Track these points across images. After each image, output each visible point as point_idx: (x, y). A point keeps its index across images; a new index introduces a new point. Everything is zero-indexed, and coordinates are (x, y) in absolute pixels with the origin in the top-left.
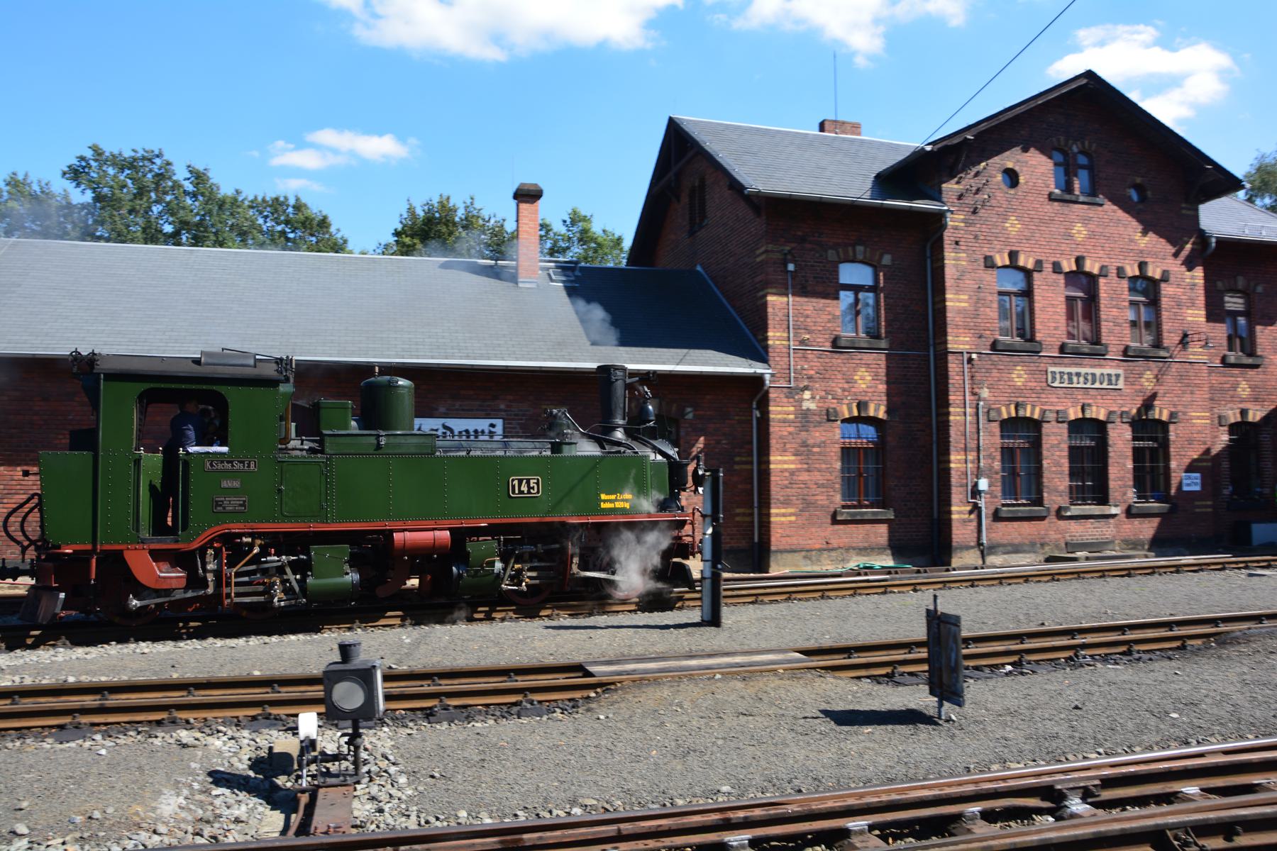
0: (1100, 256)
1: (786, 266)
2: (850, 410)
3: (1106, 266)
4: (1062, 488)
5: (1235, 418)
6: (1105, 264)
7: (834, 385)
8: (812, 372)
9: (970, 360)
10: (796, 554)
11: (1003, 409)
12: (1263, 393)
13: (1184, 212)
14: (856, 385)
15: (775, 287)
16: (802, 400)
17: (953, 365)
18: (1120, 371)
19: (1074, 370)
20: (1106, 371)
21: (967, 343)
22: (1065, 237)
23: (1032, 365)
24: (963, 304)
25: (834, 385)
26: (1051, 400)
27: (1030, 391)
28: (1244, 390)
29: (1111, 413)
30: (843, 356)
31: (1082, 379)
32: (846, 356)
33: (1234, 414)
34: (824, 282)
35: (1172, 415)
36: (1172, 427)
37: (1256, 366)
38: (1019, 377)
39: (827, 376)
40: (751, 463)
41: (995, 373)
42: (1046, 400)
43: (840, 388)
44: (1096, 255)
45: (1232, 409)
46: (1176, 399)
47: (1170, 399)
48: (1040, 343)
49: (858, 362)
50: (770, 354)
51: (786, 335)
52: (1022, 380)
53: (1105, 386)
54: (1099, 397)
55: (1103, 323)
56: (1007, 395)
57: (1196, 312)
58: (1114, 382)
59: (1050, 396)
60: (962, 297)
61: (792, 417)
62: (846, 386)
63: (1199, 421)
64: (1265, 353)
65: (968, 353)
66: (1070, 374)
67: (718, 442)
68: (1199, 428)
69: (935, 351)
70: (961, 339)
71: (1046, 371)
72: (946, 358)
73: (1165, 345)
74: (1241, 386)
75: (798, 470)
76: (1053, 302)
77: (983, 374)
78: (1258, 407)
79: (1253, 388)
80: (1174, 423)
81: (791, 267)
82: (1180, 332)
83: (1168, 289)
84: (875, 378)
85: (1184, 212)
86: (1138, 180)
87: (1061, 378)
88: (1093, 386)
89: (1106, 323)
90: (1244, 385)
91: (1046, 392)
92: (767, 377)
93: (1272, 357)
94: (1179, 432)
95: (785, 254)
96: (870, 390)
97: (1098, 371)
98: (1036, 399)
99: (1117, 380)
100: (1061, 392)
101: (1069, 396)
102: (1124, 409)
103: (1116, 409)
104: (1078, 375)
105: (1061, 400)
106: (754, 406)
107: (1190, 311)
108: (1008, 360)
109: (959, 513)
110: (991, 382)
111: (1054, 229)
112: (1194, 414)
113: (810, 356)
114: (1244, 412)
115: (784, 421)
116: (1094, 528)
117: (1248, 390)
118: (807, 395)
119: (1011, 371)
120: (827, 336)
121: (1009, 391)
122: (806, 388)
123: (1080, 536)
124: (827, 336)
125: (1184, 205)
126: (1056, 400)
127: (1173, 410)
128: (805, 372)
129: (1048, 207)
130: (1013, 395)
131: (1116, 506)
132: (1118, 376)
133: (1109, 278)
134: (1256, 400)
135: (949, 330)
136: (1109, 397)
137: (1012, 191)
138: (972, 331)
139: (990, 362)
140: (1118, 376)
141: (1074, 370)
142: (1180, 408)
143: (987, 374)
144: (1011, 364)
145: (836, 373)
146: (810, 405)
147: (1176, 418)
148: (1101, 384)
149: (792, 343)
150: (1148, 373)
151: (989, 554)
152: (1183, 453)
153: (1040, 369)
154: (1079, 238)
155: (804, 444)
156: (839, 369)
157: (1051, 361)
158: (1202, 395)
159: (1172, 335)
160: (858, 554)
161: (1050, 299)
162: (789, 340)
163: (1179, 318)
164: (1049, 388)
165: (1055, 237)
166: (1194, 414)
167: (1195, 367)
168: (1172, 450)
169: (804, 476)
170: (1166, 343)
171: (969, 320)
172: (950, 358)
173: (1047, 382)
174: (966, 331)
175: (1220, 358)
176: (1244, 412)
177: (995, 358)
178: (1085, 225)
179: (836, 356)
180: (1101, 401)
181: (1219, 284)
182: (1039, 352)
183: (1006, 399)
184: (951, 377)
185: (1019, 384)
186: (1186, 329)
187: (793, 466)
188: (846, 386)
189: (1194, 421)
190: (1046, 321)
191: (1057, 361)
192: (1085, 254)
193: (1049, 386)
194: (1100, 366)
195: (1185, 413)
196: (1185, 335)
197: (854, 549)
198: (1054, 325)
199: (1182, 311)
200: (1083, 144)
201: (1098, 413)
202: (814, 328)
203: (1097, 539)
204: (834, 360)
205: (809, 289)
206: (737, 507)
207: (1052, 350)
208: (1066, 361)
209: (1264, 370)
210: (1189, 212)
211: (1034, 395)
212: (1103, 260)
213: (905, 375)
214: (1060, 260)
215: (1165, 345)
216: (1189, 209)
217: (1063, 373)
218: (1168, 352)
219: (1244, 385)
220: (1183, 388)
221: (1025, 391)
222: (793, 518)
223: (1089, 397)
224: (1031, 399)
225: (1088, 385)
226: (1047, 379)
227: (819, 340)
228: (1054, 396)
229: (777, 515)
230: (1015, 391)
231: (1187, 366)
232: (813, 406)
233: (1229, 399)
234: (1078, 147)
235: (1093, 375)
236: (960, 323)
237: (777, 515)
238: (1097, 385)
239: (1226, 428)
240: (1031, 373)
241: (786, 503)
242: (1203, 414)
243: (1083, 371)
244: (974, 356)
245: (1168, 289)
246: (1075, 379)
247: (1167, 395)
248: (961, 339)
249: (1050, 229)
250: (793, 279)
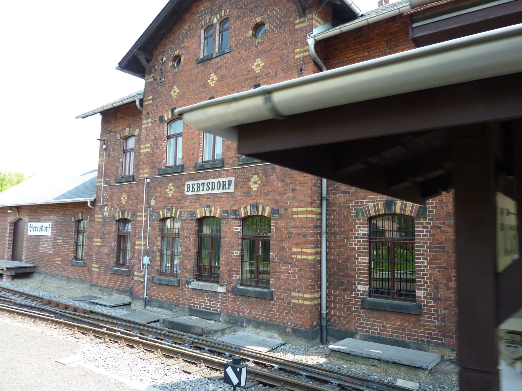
8: (108, 197)
10: (97, 288)
11: (161, 212)
29: (225, 211)
35: (274, 211)
36: (273, 223)
38: (171, 190)
53: (221, 191)
58: (227, 187)
61: (101, 220)
75: (101, 246)
87: (193, 187)
99: (229, 185)
102: (234, 208)
103: (228, 208)
116: (208, 300)
122: (106, 205)
131: (222, 286)
140: (230, 182)
146: (106, 214)
150: (255, 176)
151: (147, 306)
160: (116, 293)
187: (99, 244)
201: (215, 213)
203: (210, 309)
211: (178, 202)
222: (98, 270)
224: (175, 205)
246: (201, 188)
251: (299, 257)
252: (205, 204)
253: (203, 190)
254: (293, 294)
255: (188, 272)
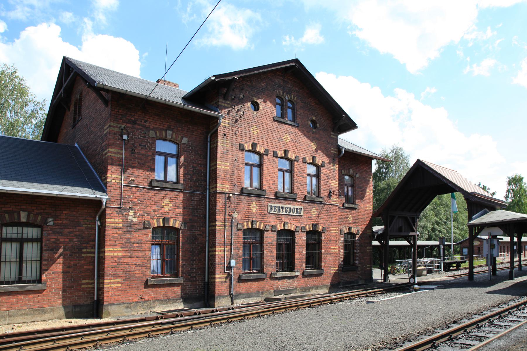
0: (295, 151)
1: (122, 137)
2: (158, 222)
3: (298, 157)
4: (273, 264)
5: (347, 231)
6: (297, 155)
7: (149, 208)
9: (229, 197)
12: (357, 220)
13: (332, 136)
14: (162, 209)
15: (114, 148)
16: (128, 215)
17: (219, 199)
18: (302, 207)
19: (281, 205)
20: (296, 207)
21: (227, 188)
22: (280, 140)
23: (261, 202)
24: (226, 168)
25: (149, 208)
26: (269, 220)
27: (259, 215)
28: (350, 219)
29: (297, 227)
30: (155, 192)
31: (284, 210)
32: (158, 192)
33: (346, 229)
34: (146, 149)
36: (323, 234)
37: (355, 209)
39: (145, 202)
40: (94, 253)
41: (241, 205)
42: (267, 220)
43: (152, 210)
44: (294, 151)
45: (345, 227)
46: (325, 221)
47: (323, 221)
48: (265, 191)
49: (165, 195)
50: (108, 187)
51: (119, 177)
52: (255, 209)
53: (295, 214)
54: (292, 219)
55: (295, 184)
56: (247, 217)
57: (335, 182)
58: (299, 212)
59: (268, 218)
60: (226, 164)
61: (121, 225)
62: (156, 209)
63: (334, 232)
64: (359, 203)
65: (227, 193)
66: (279, 207)
67: (71, 240)
68: (334, 235)
69: (209, 192)
70: (224, 186)
71: (268, 205)
72: (216, 196)
73: (322, 196)
74: (349, 217)
75: (124, 256)
76: (272, 171)
77: (235, 205)
78: (355, 226)
79: (354, 218)
80: (324, 232)
81: (125, 137)
82: (328, 191)
83: (324, 170)
84: (174, 205)
85: (332, 136)
86: (314, 118)
88: (289, 214)
89: (297, 184)
90: (350, 216)
91: (267, 216)
92: (104, 201)
93: (361, 205)
94: (326, 236)
95: (122, 129)
96: (171, 212)
97: (292, 207)
98: (262, 219)
99: (301, 211)
100: (274, 216)
101: (278, 218)
102: (303, 225)
103: (299, 225)
104: (283, 208)
105: (274, 220)
106: (97, 219)
107: (332, 181)
108: (249, 198)
109: (220, 278)
110: (240, 210)
111: (275, 135)
112: (332, 228)
113: (134, 190)
114: (350, 228)
115: (116, 228)
117: (352, 219)
118: (131, 213)
119: (250, 204)
120: (146, 180)
121: (249, 214)
122: (131, 209)
123: (281, 287)
124: (146, 180)
125: (332, 133)
126: (272, 220)
127: (324, 226)
128: (130, 199)
129: (273, 124)
130: (250, 217)
132: (301, 209)
133: (299, 162)
134: (354, 223)
135: (218, 181)
136: (296, 219)
137: (255, 113)
138: (230, 182)
139: (239, 199)
141: (281, 205)
142: (327, 226)
143: (237, 205)
144: (250, 201)
145: (151, 201)
147: (324, 230)
148: (293, 213)
149: (123, 182)
150: (314, 208)
152: (327, 246)
153: (264, 204)
154: (286, 141)
155: (129, 241)
156: (153, 199)
157: (270, 201)
158: (335, 220)
159: (325, 192)
161: (271, 169)
162: (121, 180)
163: (328, 184)
164: (268, 214)
165: (275, 139)
166: (332, 228)
167: (333, 207)
168: (322, 245)
169: (128, 260)
170: (322, 195)
171: (229, 176)
172: (218, 195)
173: (268, 211)
174: (228, 182)
175: (342, 204)
176: (350, 228)
177: (242, 197)
178: (289, 135)
179: (151, 191)
180: (293, 221)
181: (343, 171)
182: (265, 195)
183: (246, 218)
184: (217, 206)
185: (254, 211)
186: (330, 189)
187: (120, 254)
188: (156, 209)
189: (332, 231)
190: (268, 180)
191: (272, 201)
192: (289, 149)
193: (268, 212)
194: (293, 204)
195: (328, 228)
196: (330, 192)
197: (158, 300)
198: (272, 182)
199: (329, 181)
200: (291, 96)
202: (137, 174)
204: (150, 194)
205: (136, 151)
206: (83, 279)
207: (271, 195)
208: (277, 201)
209: (358, 210)
210: (334, 137)
211: (261, 217)
212: (296, 153)
213: (192, 204)
214: (277, 150)
215: (322, 196)
216: (334, 135)
217: (276, 206)
218: (323, 199)
219: (350, 216)
220: (328, 216)
221: (256, 215)
222: (120, 285)
223: (287, 219)
224: (259, 219)
225: (287, 213)
226: (268, 209)
227: (141, 181)
228: (271, 218)
229: (109, 283)
230: (251, 215)
231: (330, 206)
232: (135, 220)
233: (345, 223)
234: (288, 97)
235: (290, 208)
236: (224, 177)
237: (109, 283)
238: (291, 213)
239: (343, 235)
240: (260, 206)
241: (115, 276)
242: (336, 228)
243: (285, 206)
244: (231, 195)
245: (324, 170)
247: (322, 219)
248: (224, 186)
249: (272, 135)
250: (126, 144)
251: (334, 251)
252: (284, 221)
253: (283, 212)
254: (332, 269)
255: (272, 268)
